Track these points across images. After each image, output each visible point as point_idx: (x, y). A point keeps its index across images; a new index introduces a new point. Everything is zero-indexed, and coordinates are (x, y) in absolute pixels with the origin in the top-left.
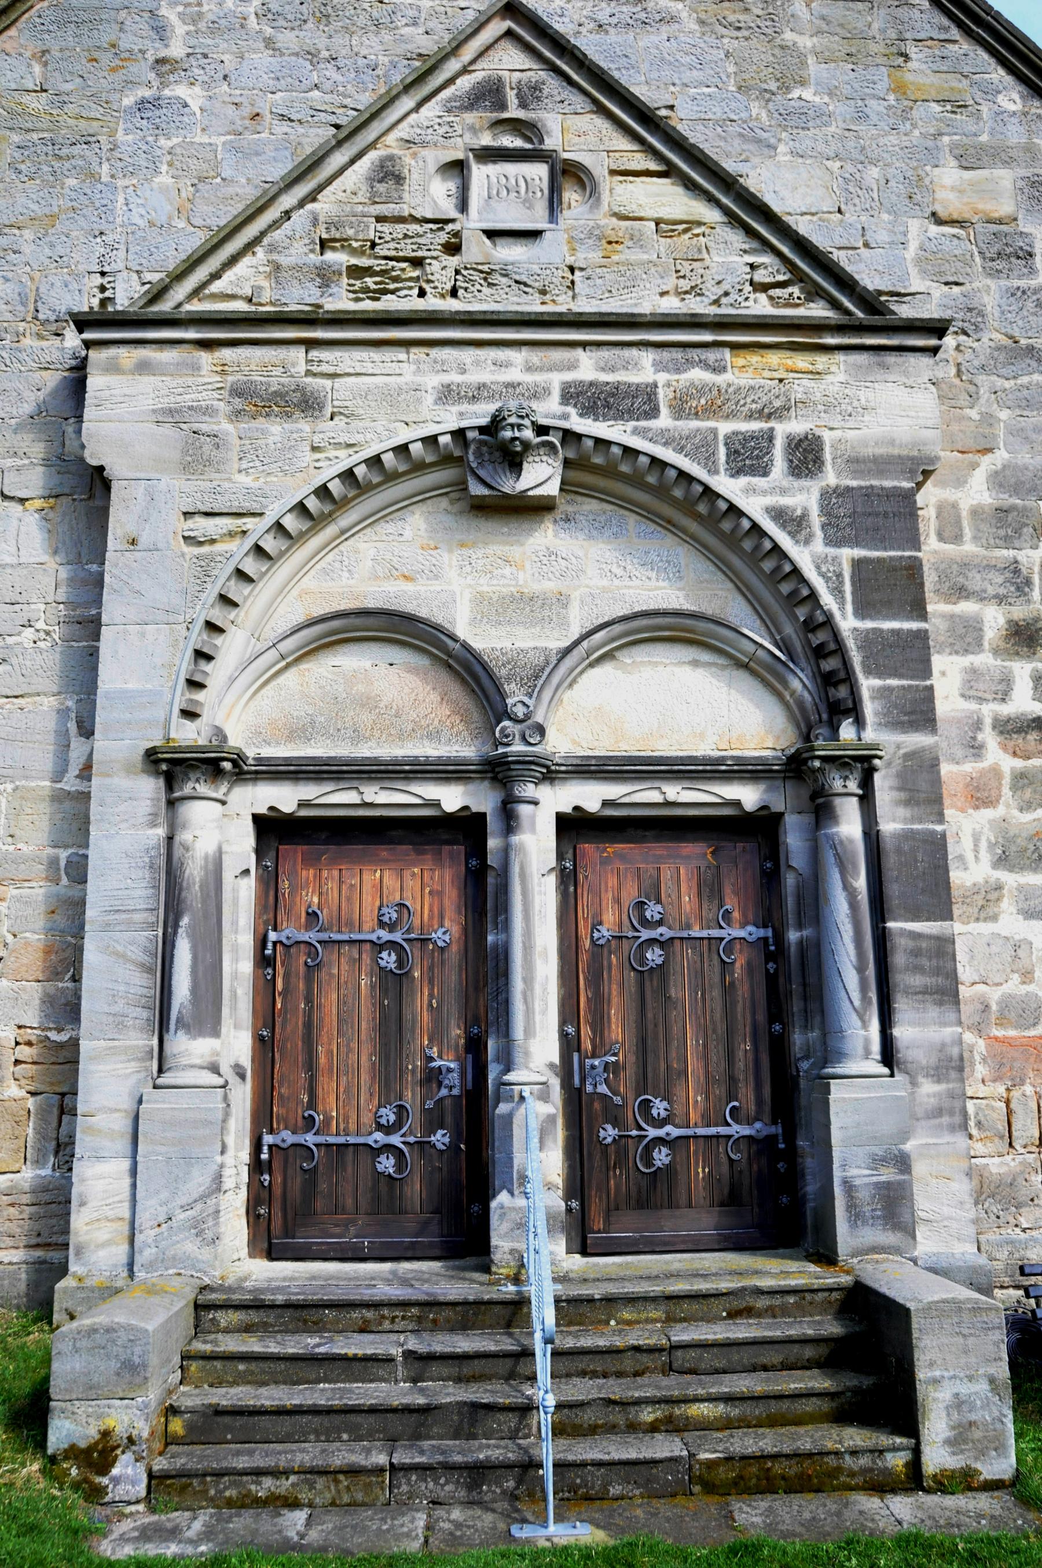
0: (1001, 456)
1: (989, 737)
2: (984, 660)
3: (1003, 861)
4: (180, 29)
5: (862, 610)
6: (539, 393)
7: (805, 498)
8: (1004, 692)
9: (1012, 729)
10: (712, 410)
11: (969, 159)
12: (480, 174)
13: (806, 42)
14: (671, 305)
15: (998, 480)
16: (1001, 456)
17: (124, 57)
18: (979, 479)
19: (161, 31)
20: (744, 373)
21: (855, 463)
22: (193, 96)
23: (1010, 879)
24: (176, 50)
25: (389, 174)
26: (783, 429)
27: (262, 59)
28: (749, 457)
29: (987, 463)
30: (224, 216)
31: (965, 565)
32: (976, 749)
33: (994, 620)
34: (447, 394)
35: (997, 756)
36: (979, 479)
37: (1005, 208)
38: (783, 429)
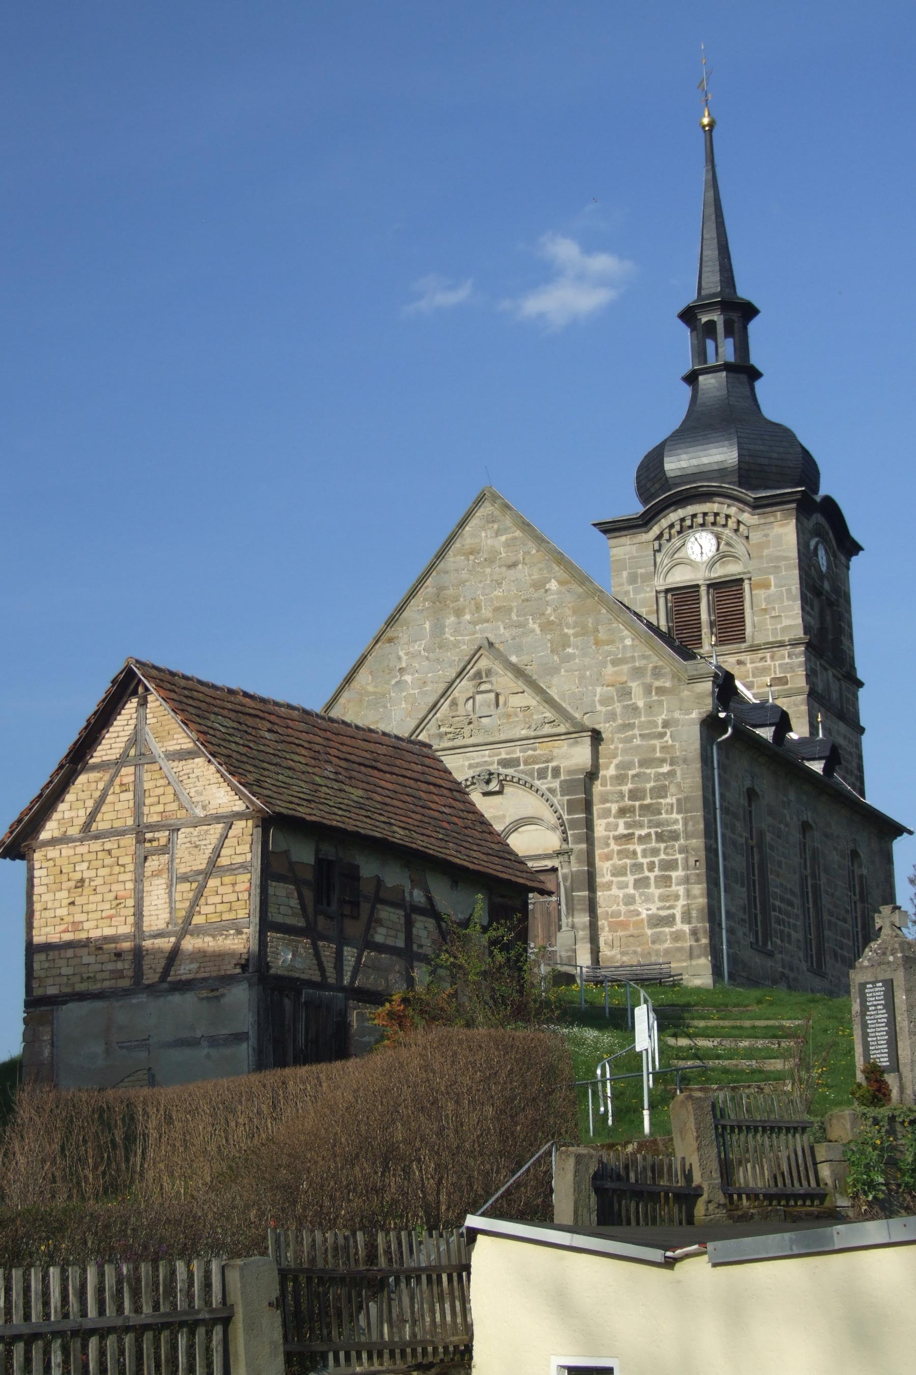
0: (619, 758)
1: (612, 842)
2: (611, 820)
3: (613, 875)
4: (404, 658)
5: (568, 814)
6: (492, 763)
7: (556, 784)
8: (616, 826)
9: (617, 838)
10: (535, 762)
11: (614, 663)
12: (479, 698)
13: (570, 632)
14: (524, 733)
15: (617, 767)
16: (619, 758)
17: (391, 670)
18: (612, 766)
19: (399, 658)
20: (541, 750)
21: (570, 772)
22: (408, 678)
23: (614, 879)
24: (404, 665)
25: (454, 704)
26: (551, 765)
27: (425, 663)
28: (542, 774)
29: (615, 762)
30: (421, 716)
31: (607, 793)
32: (608, 845)
33: (614, 807)
34: (471, 766)
35: (614, 847)
36: (612, 766)
37: (624, 679)
38: (551, 765)
